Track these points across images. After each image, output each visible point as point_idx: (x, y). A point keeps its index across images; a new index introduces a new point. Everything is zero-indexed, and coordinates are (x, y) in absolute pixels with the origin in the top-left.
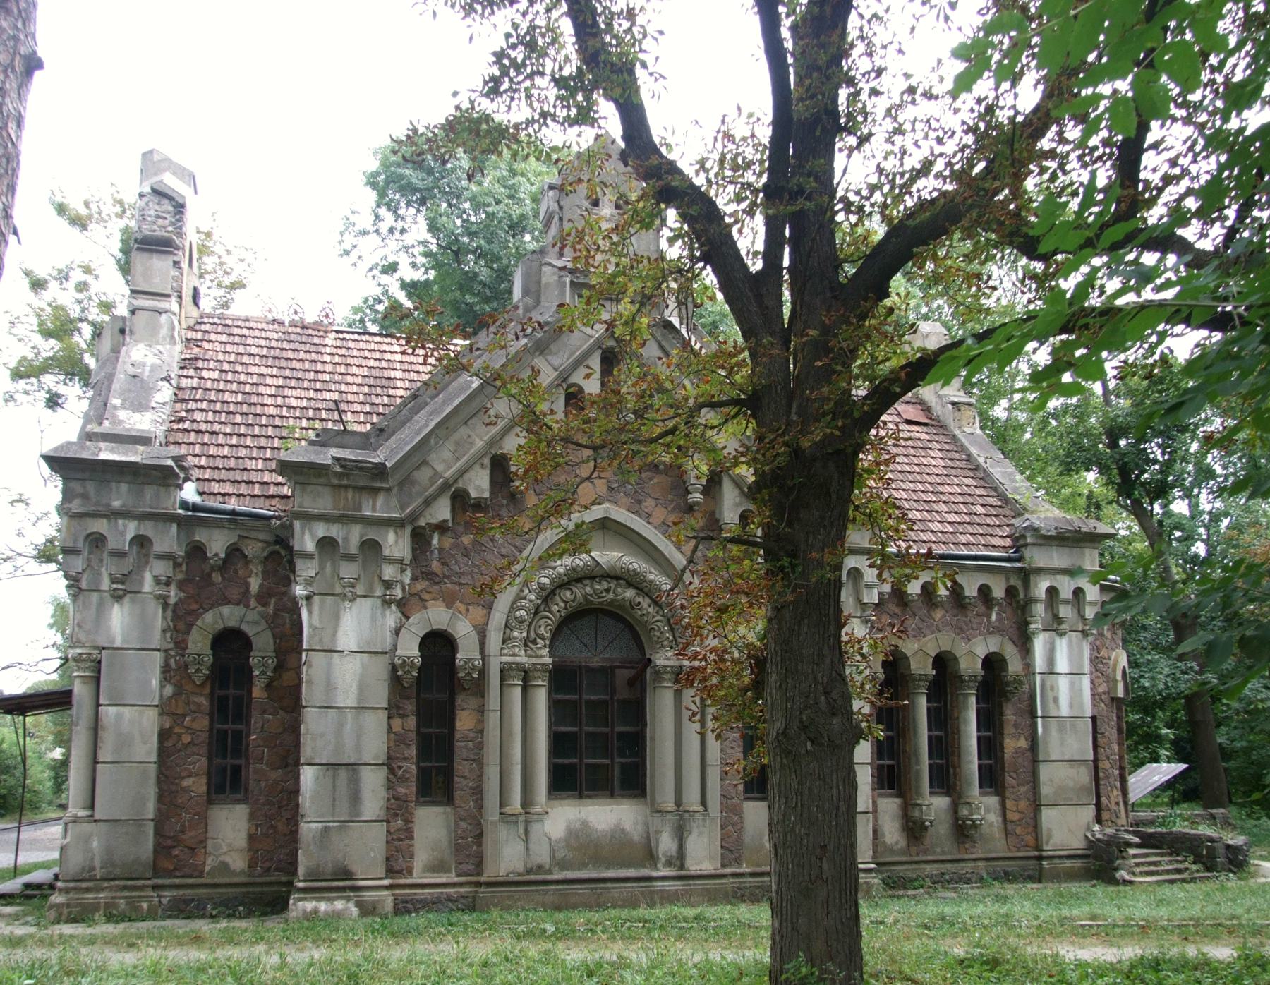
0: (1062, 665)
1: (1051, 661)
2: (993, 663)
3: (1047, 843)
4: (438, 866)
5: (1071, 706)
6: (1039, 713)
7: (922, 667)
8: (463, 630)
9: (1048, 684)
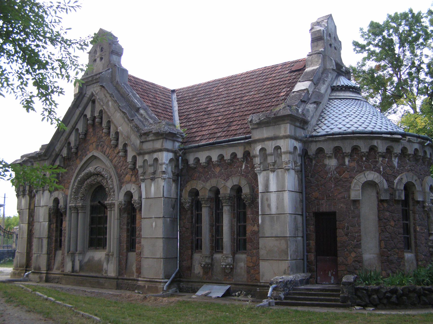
0: (273, 187)
1: (267, 186)
3: (262, 280)
4: (58, 269)
5: (277, 208)
6: (260, 213)
8: (61, 198)
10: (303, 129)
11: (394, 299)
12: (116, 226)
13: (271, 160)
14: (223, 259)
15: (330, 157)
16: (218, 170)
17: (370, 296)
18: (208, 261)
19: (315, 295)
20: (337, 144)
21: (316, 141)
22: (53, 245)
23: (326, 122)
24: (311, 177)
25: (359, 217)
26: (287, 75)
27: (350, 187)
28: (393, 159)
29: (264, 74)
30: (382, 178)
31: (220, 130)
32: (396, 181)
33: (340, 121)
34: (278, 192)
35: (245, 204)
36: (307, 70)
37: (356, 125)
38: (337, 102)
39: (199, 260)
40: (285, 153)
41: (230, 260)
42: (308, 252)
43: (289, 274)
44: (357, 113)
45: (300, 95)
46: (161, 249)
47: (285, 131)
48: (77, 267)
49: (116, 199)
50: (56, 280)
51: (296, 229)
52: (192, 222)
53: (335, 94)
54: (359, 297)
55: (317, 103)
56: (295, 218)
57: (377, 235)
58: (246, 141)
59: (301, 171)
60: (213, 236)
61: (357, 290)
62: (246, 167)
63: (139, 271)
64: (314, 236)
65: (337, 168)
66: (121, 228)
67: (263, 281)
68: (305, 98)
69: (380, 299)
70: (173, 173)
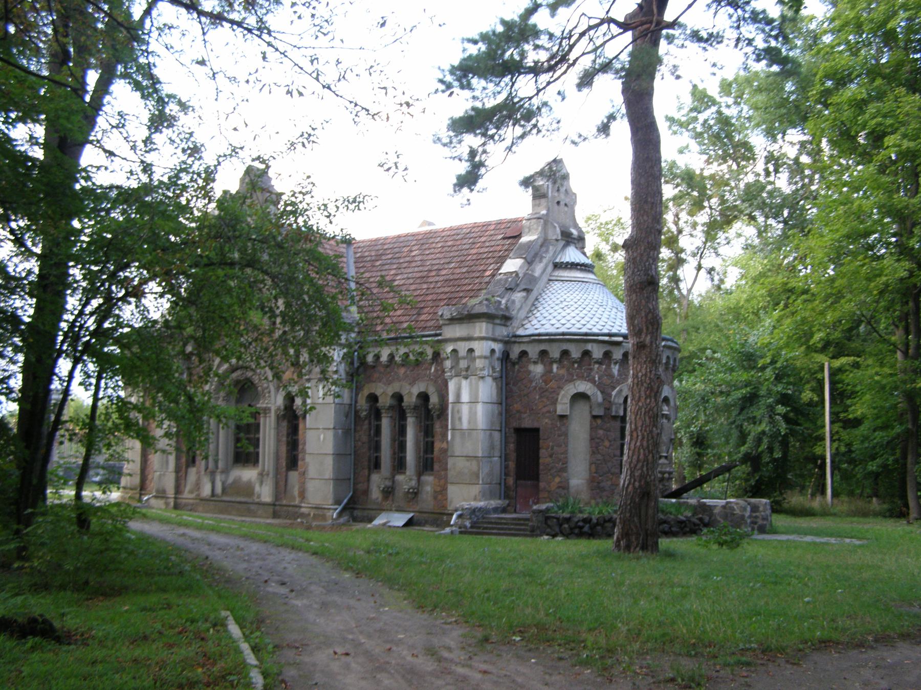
0: (465, 397)
1: (458, 395)
2: (424, 397)
4: (191, 492)
5: (469, 422)
6: (450, 427)
7: (385, 401)
9: (456, 409)
10: (505, 325)
11: (586, 528)
12: (272, 437)
13: (463, 364)
14: (406, 481)
15: (535, 363)
16: (402, 371)
17: (561, 525)
18: (388, 483)
19: (505, 524)
20: (543, 347)
21: (520, 343)
22: (184, 460)
23: (538, 315)
24: (514, 385)
25: (566, 435)
26: (498, 243)
27: (557, 399)
28: (612, 366)
29: (472, 235)
30: (596, 390)
31: (407, 318)
32: (614, 393)
33: (555, 314)
34: (472, 403)
35: (432, 414)
36: (524, 239)
37: (573, 321)
38: (558, 285)
39: (377, 482)
40: (480, 357)
41: (413, 483)
42: (506, 475)
43: (480, 501)
44: (579, 303)
45: (506, 280)
46: (331, 468)
47: (481, 331)
48: (219, 489)
49: (273, 401)
50: (190, 507)
51: (492, 447)
52: (370, 435)
53: (556, 273)
54: (549, 526)
55: (528, 291)
56: (491, 435)
57: (588, 457)
58: (436, 338)
59: (501, 377)
60: (394, 453)
61: (547, 518)
62: (436, 370)
63: (302, 494)
64: (513, 456)
65: (542, 377)
66: (278, 441)
67: (450, 508)
68: (512, 284)
69: (571, 529)
70: (347, 373)
